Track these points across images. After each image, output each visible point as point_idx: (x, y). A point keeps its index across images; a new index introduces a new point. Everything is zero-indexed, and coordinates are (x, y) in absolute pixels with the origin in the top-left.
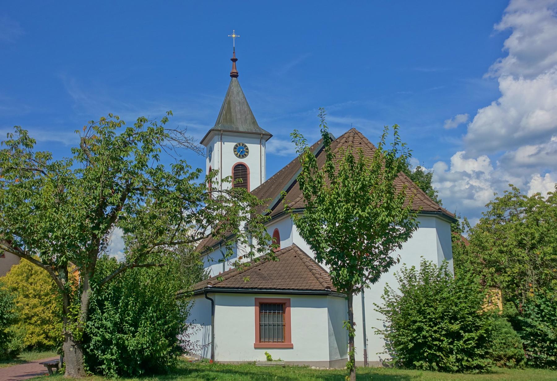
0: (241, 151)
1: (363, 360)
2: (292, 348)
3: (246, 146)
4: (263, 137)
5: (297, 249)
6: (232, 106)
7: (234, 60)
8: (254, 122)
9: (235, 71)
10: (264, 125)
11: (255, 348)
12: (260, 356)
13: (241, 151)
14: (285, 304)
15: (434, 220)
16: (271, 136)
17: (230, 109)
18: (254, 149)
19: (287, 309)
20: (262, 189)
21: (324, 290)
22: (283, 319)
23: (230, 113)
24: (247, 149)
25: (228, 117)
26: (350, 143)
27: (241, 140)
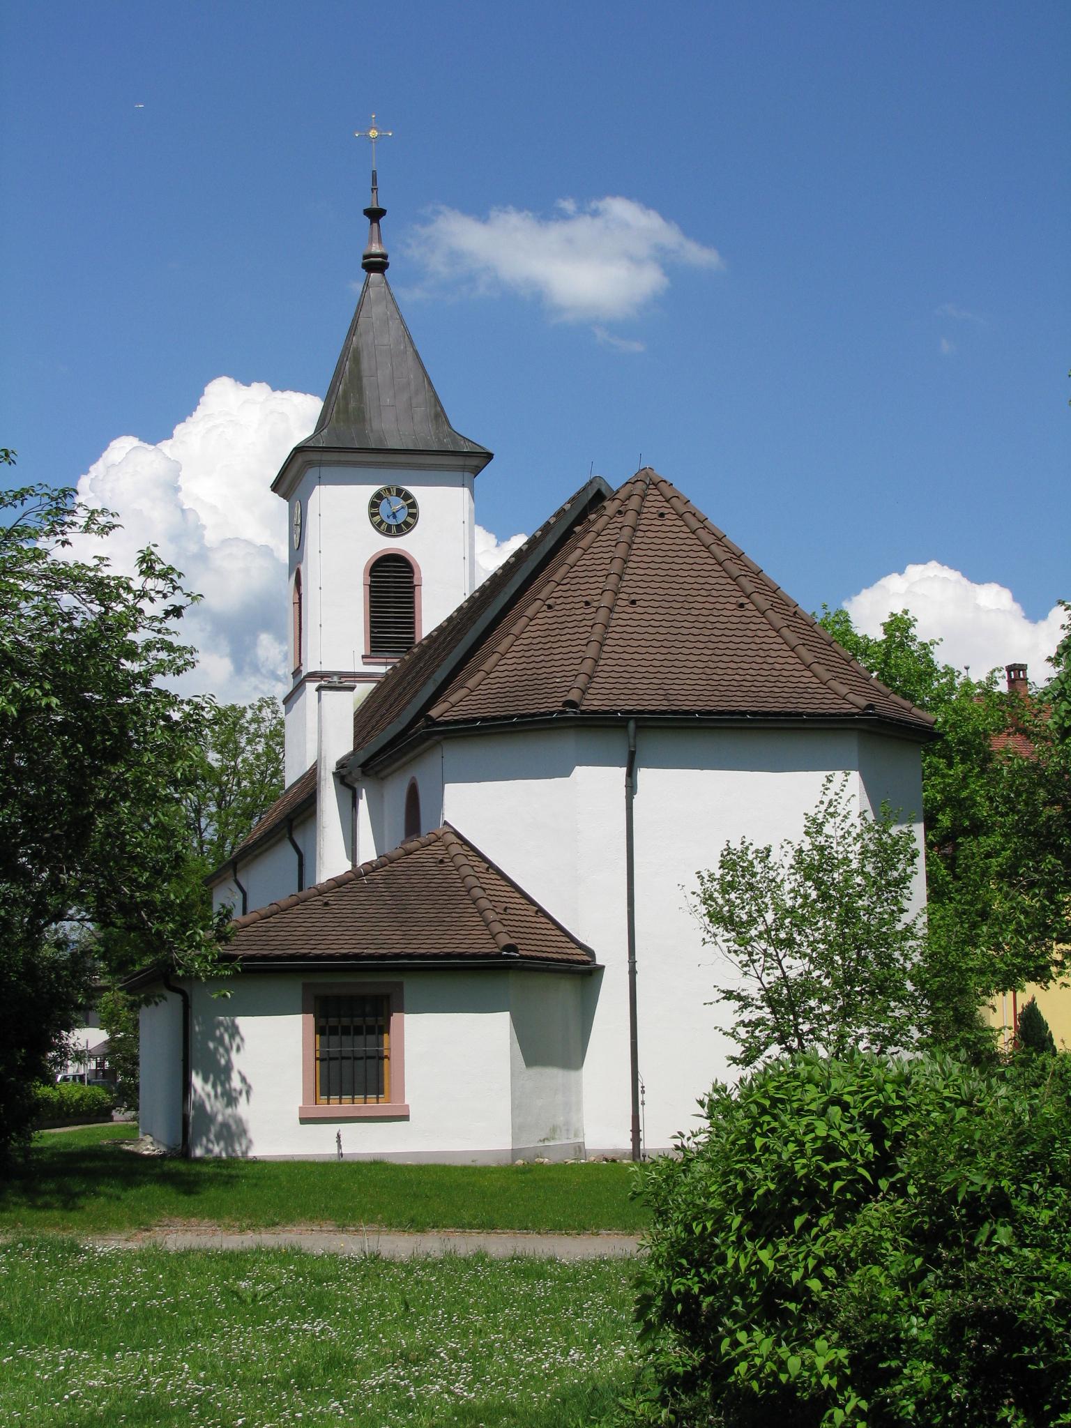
0: (395, 516)
1: (629, 1146)
2: (405, 1118)
3: (407, 496)
4: (466, 462)
5: (453, 838)
6: (365, 365)
7: (375, 215)
8: (439, 416)
9: (376, 249)
10: (470, 425)
11: (304, 1121)
12: (318, 1144)
13: (395, 516)
14: (388, 997)
15: (850, 745)
16: (489, 456)
17: (360, 378)
18: (442, 505)
19: (395, 1017)
20: (438, 637)
21: (499, 956)
22: (380, 1043)
23: (360, 390)
24: (413, 505)
25: (352, 404)
26: (631, 515)
27: (393, 477)
